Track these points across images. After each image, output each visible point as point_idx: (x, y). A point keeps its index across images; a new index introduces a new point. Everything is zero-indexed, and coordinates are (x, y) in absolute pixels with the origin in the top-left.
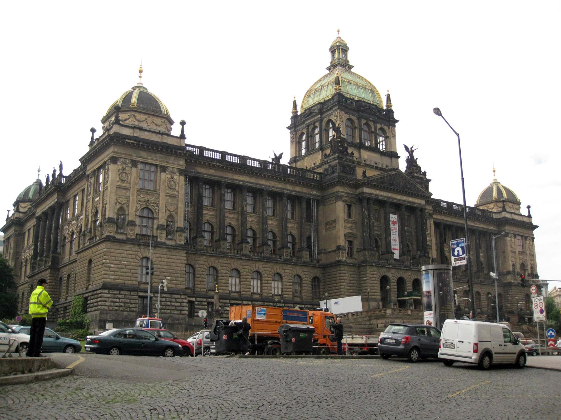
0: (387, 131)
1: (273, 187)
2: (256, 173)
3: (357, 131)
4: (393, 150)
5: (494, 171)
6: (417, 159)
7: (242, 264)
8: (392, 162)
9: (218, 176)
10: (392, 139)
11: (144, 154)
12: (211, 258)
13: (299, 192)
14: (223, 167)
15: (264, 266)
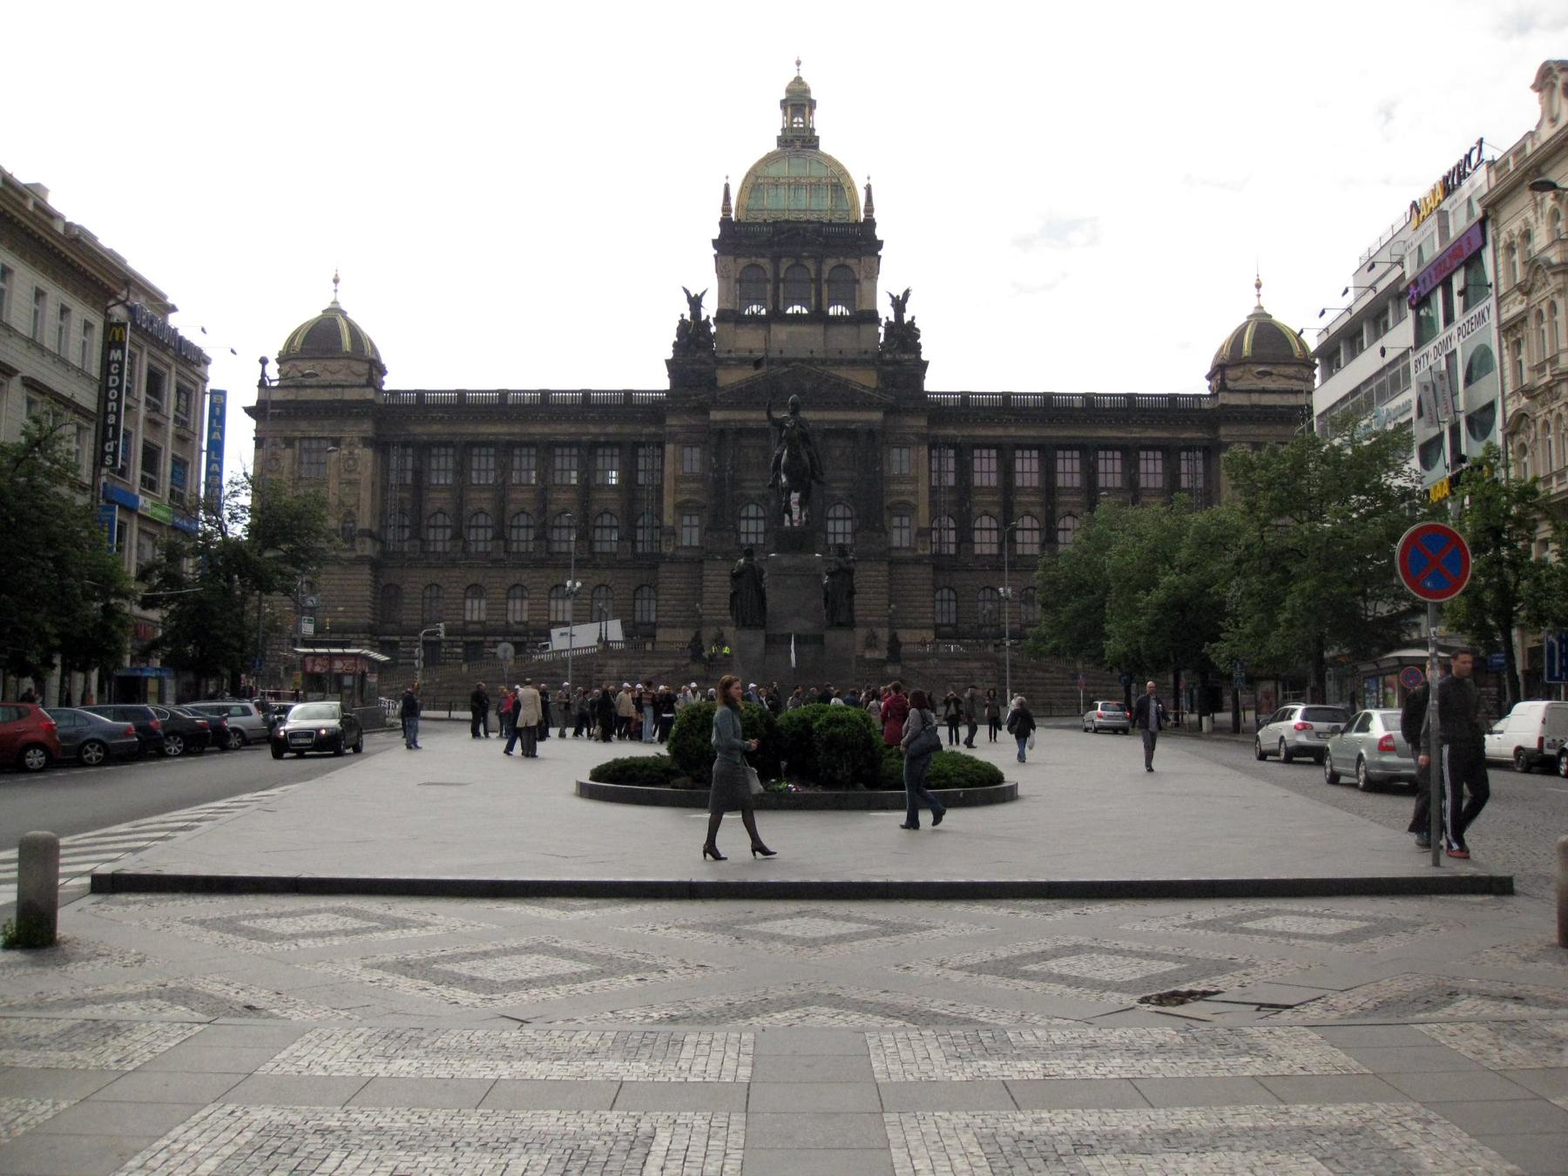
0: (855, 268)
3: (769, 287)
4: (865, 307)
5: (1258, 286)
10: (865, 285)
11: (303, 425)
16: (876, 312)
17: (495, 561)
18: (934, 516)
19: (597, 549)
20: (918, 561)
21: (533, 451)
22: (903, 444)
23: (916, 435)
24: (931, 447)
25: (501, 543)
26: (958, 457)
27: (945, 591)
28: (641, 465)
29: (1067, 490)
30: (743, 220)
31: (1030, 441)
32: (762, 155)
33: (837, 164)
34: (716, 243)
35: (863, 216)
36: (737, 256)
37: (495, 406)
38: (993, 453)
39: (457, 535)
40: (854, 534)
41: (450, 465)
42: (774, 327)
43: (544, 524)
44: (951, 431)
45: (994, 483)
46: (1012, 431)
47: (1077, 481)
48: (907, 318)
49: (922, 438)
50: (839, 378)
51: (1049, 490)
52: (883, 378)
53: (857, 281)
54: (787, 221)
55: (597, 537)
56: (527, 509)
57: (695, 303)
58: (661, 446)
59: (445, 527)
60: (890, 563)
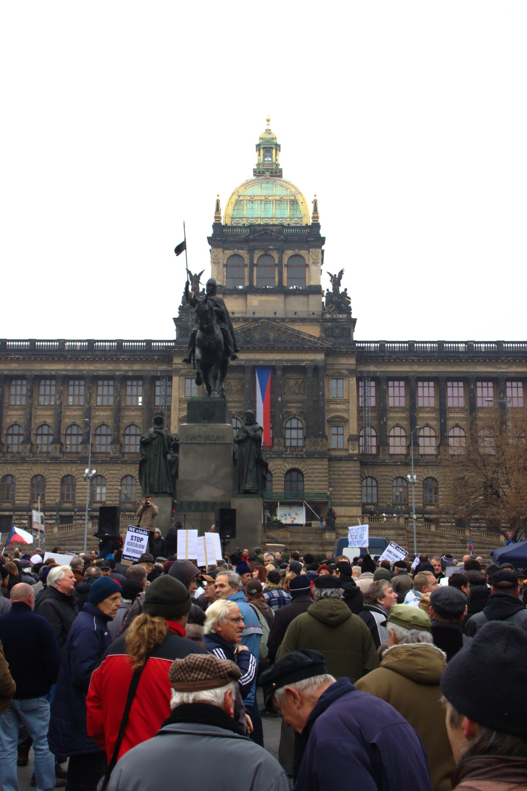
0: (306, 257)
1: (98, 371)
2: (70, 358)
3: (247, 270)
4: (312, 283)
6: (346, 290)
7: (48, 468)
8: (308, 301)
9: (21, 370)
10: (313, 268)
12: (7, 465)
13: (138, 371)
14: (24, 359)
15: (78, 468)
16: (320, 287)
17: (52, 458)
18: (361, 427)
19: (126, 450)
20: (349, 458)
21: (82, 383)
22: (339, 376)
23: (348, 369)
24: (359, 380)
25: (58, 446)
26: (377, 387)
27: (369, 480)
28: (158, 392)
29: (453, 409)
30: (229, 224)
31: (427, 375)
32: (243, 181)
33: (293, 186)
34: (209, 238)
35: (311, 221)
36: (225, 249)
37: (56, 351)
38: (402, 383)
39: (27, 440)
40: (304, 438)
41: (24, 392)
42: (249, 297)
43: (88, 433)
44: (372, 368)
45: (403, 404)
46: (416, 368)
47: (462, 403)
48: (341, 290)
49: (352, 372)
50: (294, 330)
51: (442, 409)
52: (324, 330)
53: (307, 266)
54: (259, 225)
55: (127, 442)
56: (78, 422)
57: (195, 279)
58: (170, 379)
59: (19, 435)
60: (331, 459)
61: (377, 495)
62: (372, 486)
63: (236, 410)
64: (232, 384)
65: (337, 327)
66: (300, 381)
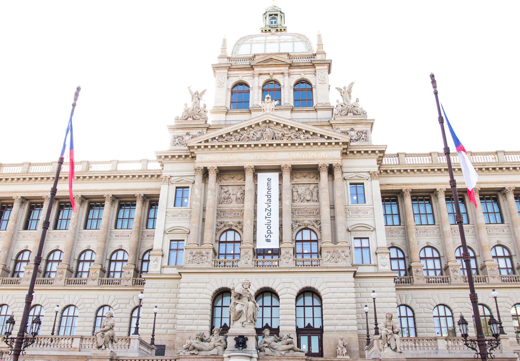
6: (357, 100)
48: (353, 101)
49: (372, 175)
57: (197, 96)
61: (415, 328)
62: (407, 317)
63: (234, 220)
64: (231, 192)
65: (352, 130)
66: (312, 187)
